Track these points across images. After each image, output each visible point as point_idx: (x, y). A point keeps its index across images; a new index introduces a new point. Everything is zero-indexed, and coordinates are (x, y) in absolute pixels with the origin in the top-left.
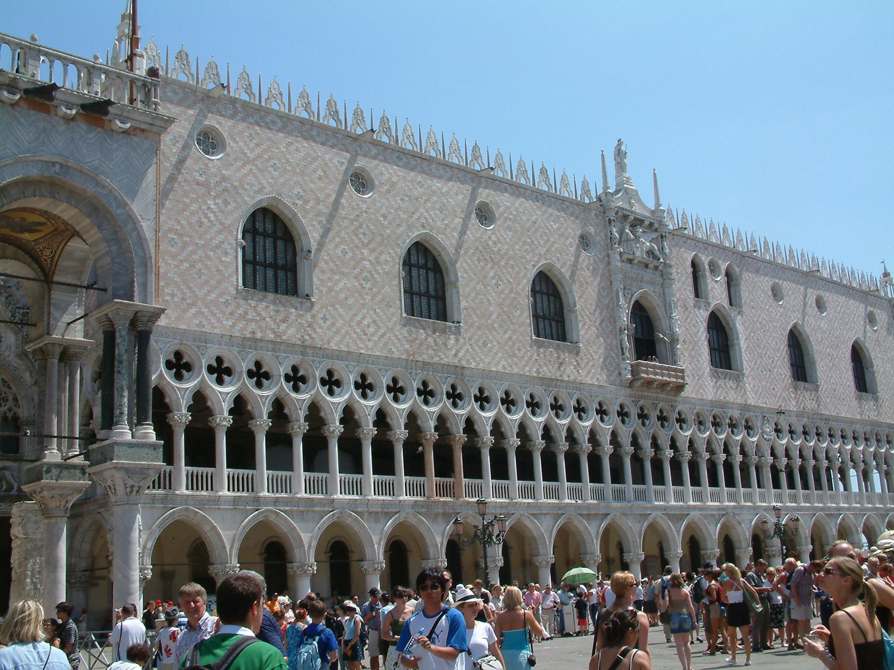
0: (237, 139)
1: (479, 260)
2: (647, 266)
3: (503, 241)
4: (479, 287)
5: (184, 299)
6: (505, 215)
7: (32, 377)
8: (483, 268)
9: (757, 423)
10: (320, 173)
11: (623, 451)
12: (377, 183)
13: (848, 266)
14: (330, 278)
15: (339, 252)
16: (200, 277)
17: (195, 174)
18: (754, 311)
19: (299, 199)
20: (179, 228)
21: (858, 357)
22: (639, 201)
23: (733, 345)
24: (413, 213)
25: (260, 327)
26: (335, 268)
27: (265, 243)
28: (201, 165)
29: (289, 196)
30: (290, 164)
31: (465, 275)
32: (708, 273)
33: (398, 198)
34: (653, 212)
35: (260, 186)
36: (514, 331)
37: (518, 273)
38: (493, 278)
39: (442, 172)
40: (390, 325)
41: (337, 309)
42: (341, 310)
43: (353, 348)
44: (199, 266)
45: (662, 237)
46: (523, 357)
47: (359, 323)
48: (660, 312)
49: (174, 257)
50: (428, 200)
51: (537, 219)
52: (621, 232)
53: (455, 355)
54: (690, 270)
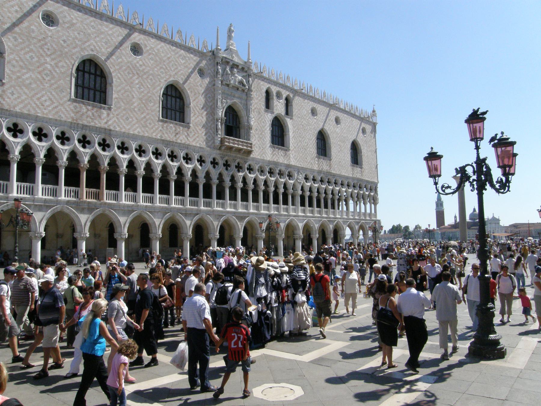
1: (129, 73)
2: (238, 89)
3: (146, 64)
6: (150, 52)
8: (131, 78)
12: (61, 21)
13: (355, 105)
14: (19, 71)
15: (28, 57)
18: (299, 119)
21: (355, 148)
22: (238, 56)
24: (86, 42)
26: (24, 66)
31: (118, 80)
32: (275, 98)
34: (245, 62)
36: (148, 114)
37: (155, 83)
38: (137, 84)
40: (61, 102)
41: (22, 89)
42: (26, 91)
43: (33, 112)
45: (249, 75)
46: (152, 128)
47: (38, 99)
50: (98, 36)
51: (171, 56)
52: (224, 70)
53: (106, 123)
54: (264, 95)
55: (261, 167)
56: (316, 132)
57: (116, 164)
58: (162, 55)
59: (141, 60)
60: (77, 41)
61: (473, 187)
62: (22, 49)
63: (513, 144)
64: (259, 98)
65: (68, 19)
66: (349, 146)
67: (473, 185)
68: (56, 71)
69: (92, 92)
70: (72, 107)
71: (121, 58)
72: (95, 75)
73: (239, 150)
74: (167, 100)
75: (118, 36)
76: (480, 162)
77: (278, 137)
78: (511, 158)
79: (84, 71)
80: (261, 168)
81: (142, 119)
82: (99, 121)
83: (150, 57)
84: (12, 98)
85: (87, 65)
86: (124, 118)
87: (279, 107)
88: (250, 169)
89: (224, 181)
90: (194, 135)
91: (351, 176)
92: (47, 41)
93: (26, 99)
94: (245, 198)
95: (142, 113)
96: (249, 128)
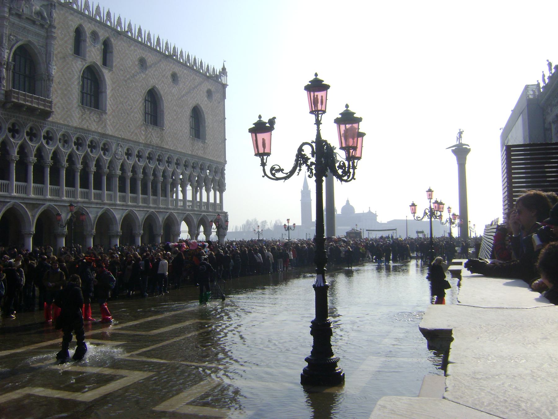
18: (122, 72)
21: (197, 114)
23: (102, 93)
32: (88, 40)
54: (73, 34)
55: (64, 135)
56: (144, 92)
61: (311, 172)
63: (359, 120)
67: (312, 170)
73: (31, 111)
76: (319, 142)
77: (91, 96)
78: (355, 139)
87: (94, 54)
88: (49, 138)
91: (190, 153)
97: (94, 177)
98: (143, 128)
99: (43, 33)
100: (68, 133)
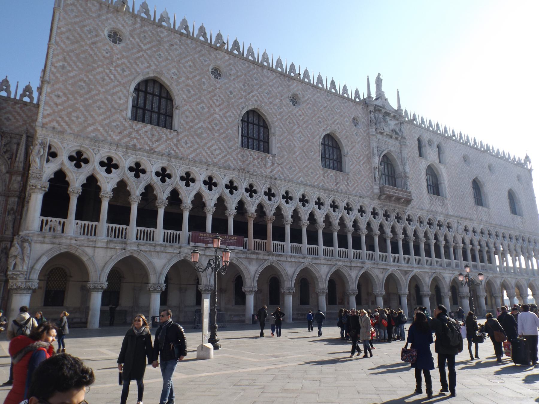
0: (136, 37)
1: (290, 123)
2: (391, 137)
4: (290, 137)
5: (85, 121)
7: (6, 168)
8: (292, 127)
9: (454, 226)
10: (190, 63)
11: (374, 233)
14: (191, 122)
16: (99, 109)
17: (103, 51)
18: (453, 167)
19: (175, 75)
20: (87, 80)
21: (512, 196)
23: (441, 184)
24: (249, 93)
25: (139, 143)
27: (153, 99)
28: (107, 47)
29: (167, 73)
30: (171, 56)
31: (280, 130)
33: (241, 84)
35: (148, 65)
36: (309, 163)
37: (313, 133)
38: (298, 133)
39: (270, 74)
41: (195, 138)
42: (197, 139)
44: (99, 103)
46: (314, 177)
47: (209, 148)
48: (399, 162)
49: (81, 96)
50: (261, 87)
53: (271, 172)
54: (417, 142)
55: (419, 218)
56: (471, 180)
57: (282, 215)
58: (319, 105)
59: (300, 110)
60: (242, 92)
62: (194, 101)
64: (412, 146)
65: (234, 71)
66: (506, 194)
68: (224, 122)
69: (256, 142)
70: (239, 156)
71: (282, 108)
72: (259, 125)
73: (398, 199)
74: (325, 150)
75: (278, 87)
77: (433, 187)
79: (248, 122)
80: (420, 219)
81: (304, 168)
82: (264, 170)
83: (308, 107)
84: (186, 147)
85: (251, 116)
86: (288, 167)
87: (432, 156)
89: (385, 233)
90: (354, 184)
92: (216, 92)
93: (198, 148)
94: (407, 251)
95: (304, 163)
96: (406, 176)
97: (440, 250)
98: (474, 209)
99: (397, 143)
100: (423, 216)
